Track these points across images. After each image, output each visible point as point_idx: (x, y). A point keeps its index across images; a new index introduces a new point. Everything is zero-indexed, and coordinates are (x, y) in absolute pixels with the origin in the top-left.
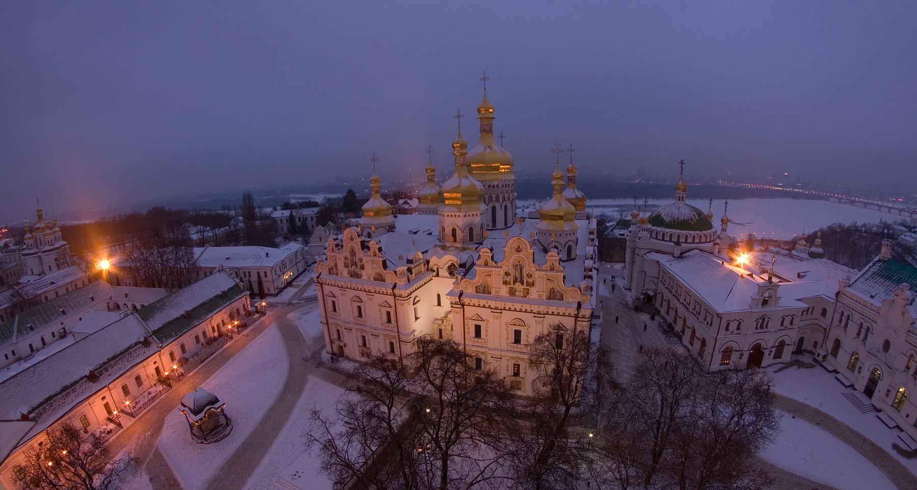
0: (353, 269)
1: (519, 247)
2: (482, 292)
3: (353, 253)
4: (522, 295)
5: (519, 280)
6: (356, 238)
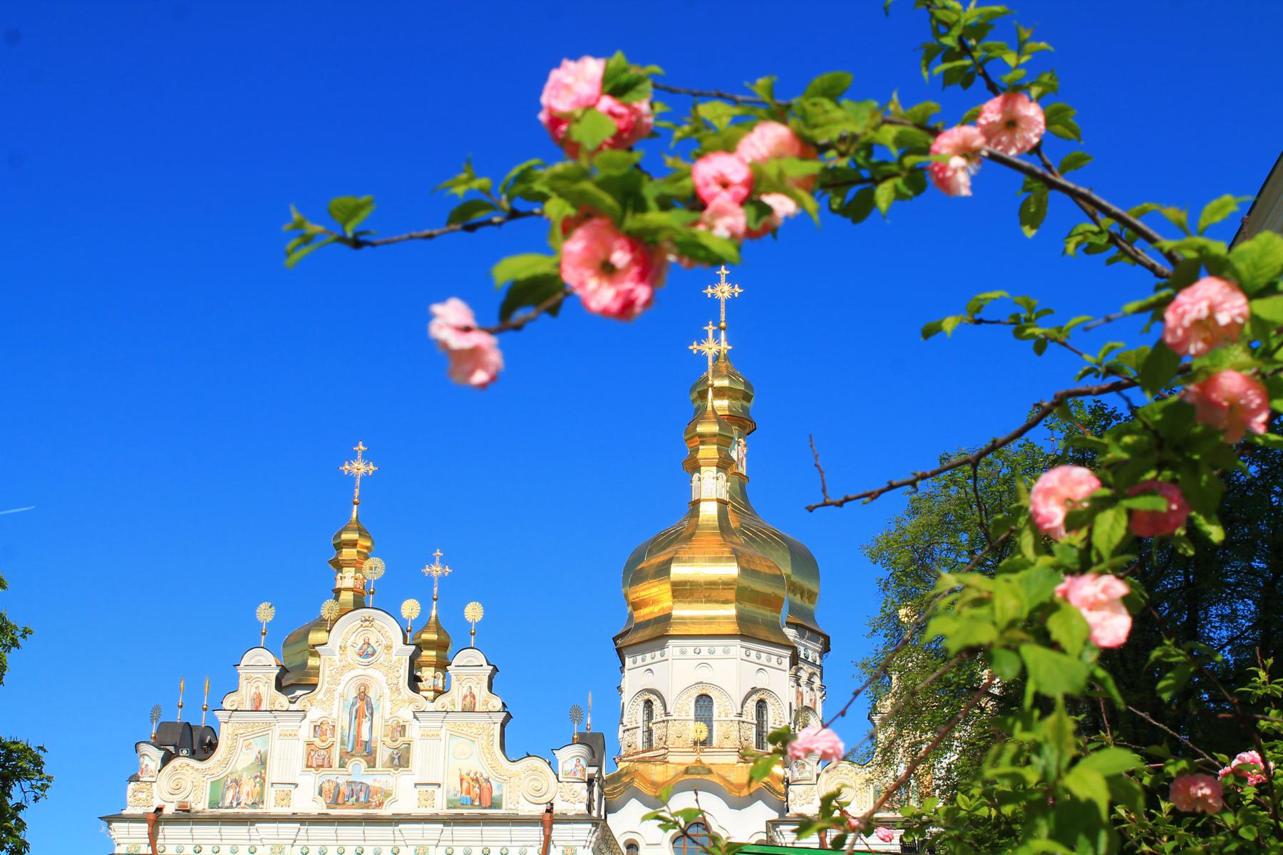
0: (357, 770)
3: (363, 704)
6: (389, 647)
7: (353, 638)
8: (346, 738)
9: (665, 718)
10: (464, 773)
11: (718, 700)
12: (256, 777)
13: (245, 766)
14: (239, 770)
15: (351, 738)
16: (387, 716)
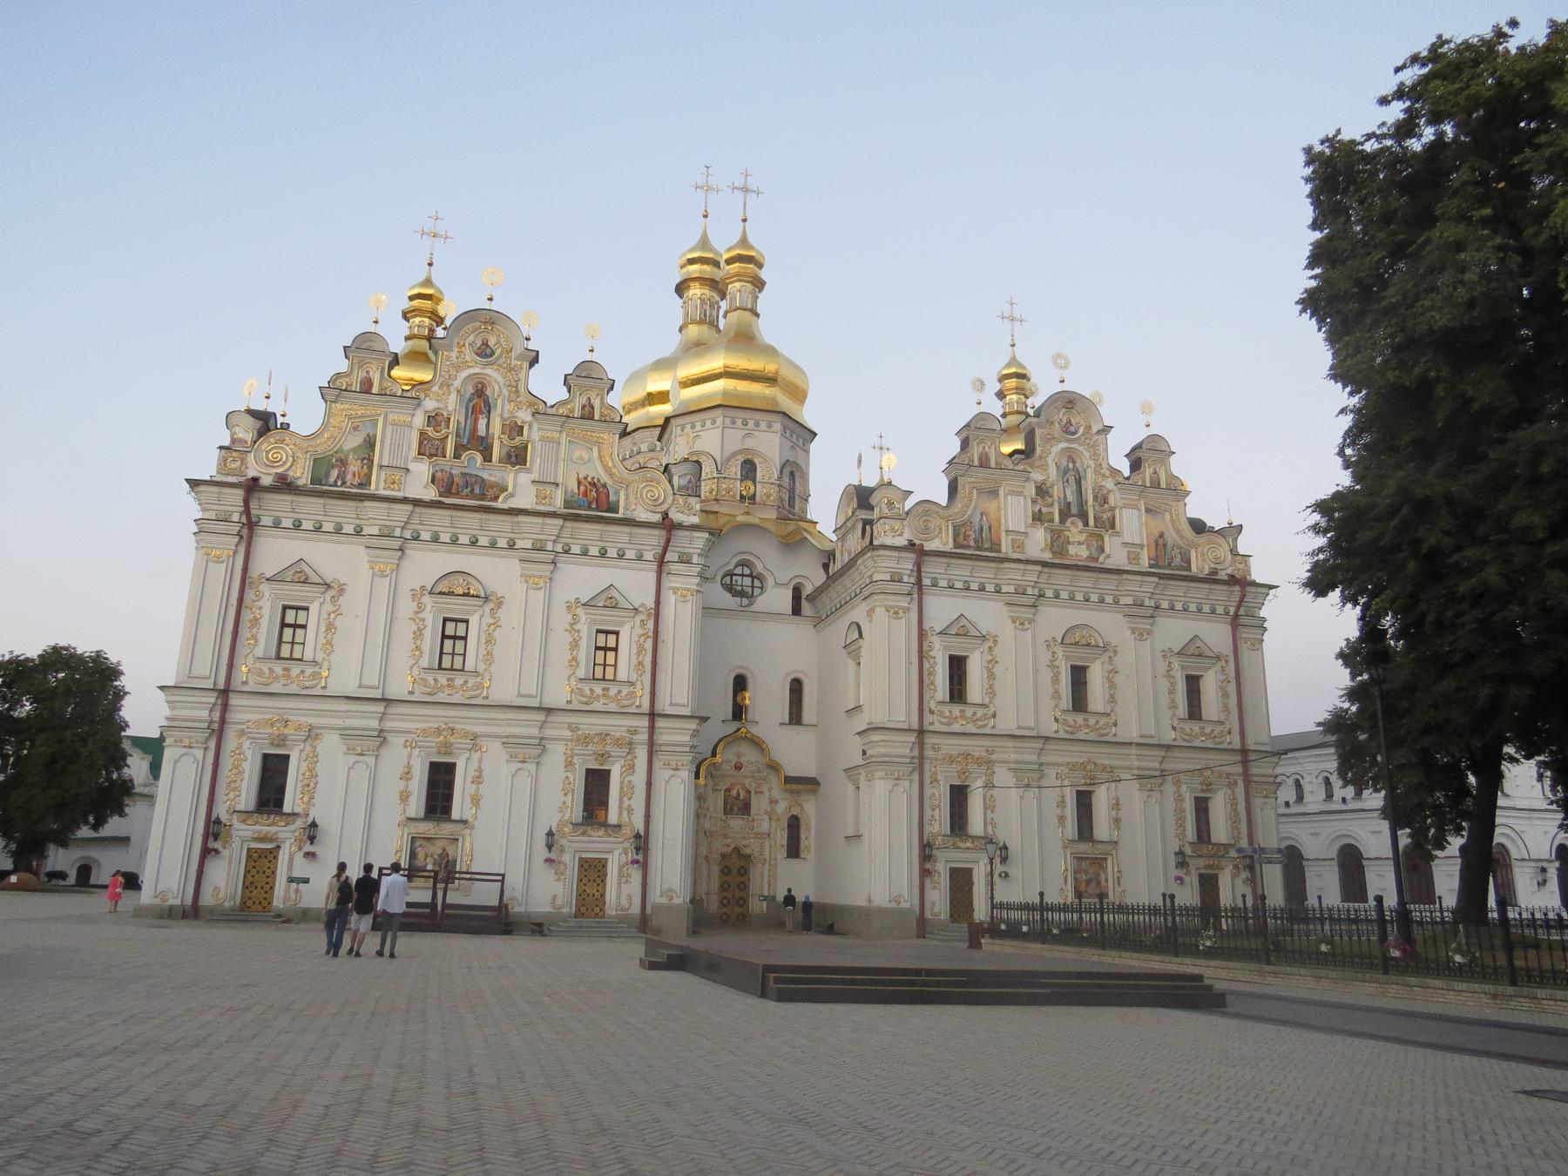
1: (1069, 422)
2: (972, 543)
3: (479, 400)
4: (1085, 554)
5: (1074, 511)
7: (471, 338)
8: (462, 432)
9: (715, 475)
10: (581, 477)
11: (762, 465)
12: (364, 459)
13: (352, 447)
14: (345, 449)
15: (467, 432)
16: (506, 416)
